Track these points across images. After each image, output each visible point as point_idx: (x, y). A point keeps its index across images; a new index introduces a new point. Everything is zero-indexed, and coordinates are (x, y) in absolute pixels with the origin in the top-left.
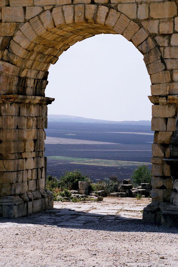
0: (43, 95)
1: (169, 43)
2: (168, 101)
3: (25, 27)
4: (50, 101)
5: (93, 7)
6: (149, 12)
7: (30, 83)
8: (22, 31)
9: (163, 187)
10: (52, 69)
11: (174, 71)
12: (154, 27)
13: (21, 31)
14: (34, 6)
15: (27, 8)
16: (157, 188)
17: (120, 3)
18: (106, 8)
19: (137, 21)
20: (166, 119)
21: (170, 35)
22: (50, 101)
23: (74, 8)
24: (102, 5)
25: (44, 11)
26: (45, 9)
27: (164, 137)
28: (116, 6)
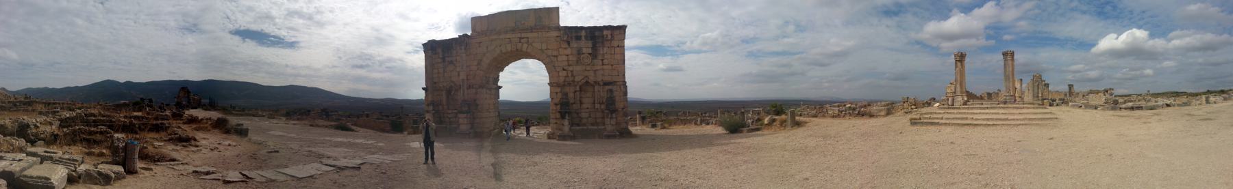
0: (497, 85)
4: (501, 87)
5: (520, 44)
7: (491, 80)
9: (556, 123)
10: (501, 74)
12: (549, 53)
19: (541, 50)
20: (557, 93)
21: (557, 56)
22: (501, 87)
27: (557, 101)
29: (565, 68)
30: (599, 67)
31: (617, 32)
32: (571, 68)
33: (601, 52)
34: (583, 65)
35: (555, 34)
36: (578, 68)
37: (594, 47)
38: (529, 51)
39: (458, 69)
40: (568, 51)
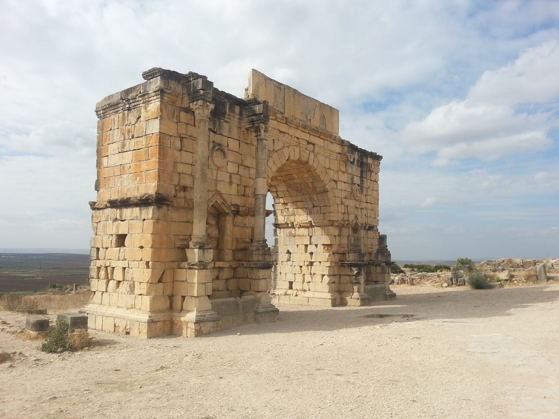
1: (337, 187)
2: (339, 225)
3: (275, 155)
6: (330, 165)
8: (273, 158)
9: (334, 282)
11: (339, 205)
12: (332, 174)
13: (272, 159)
14: (279, 140)
15: (275, 141)
16: (331, 283)
17: (318, 153)
18: (314, 155)
19: (325, 167)
20: (334, 236)
21: (336, 182)
23: (300, 150)
24: (311, 152)
25: (284, 147)
26: (285, 146)
28: (317, 155)
29: (344, 200)
30: (364, 205)
31: (376, 162)
32: (346, 202)
33: (365, 185)
34: (355, 199)
35: (337, 148)
36: (351, 203)
37: (361, 177)
38: (315, 165)
39: (232, 168)
40: (345, 177)
